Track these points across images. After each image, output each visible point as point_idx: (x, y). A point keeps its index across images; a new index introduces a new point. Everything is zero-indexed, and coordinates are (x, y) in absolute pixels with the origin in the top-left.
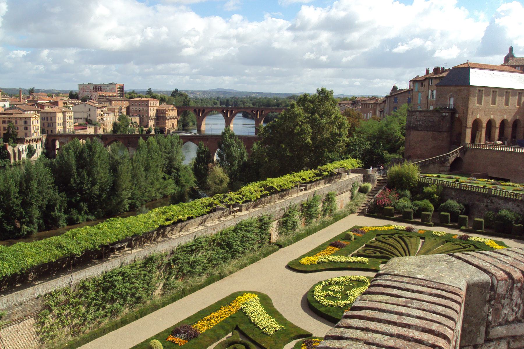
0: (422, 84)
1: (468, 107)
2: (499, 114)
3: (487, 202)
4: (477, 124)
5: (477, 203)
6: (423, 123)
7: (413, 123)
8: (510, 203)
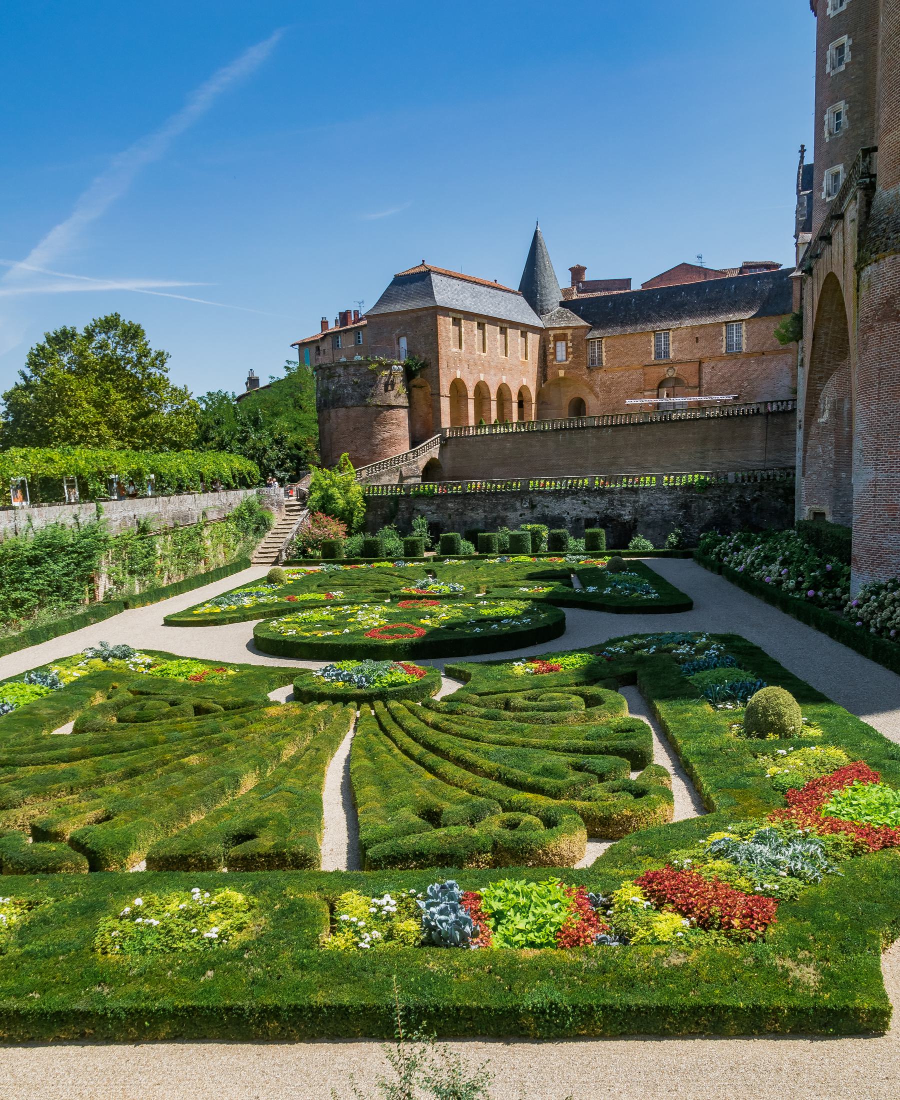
0: (318, 348)
1: (438, 353)
2: (493, 371)
3: (523, 508)
5: (502, 514)
6: (354, 390)
7: (335, 391)
8: (568, 499)
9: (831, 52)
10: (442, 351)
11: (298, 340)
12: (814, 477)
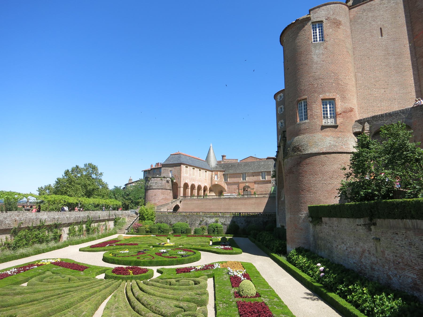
4: (186, 185)
9: (279, 109)
10: (182, 175)
11: (144, 170)
12: (281, 215)
